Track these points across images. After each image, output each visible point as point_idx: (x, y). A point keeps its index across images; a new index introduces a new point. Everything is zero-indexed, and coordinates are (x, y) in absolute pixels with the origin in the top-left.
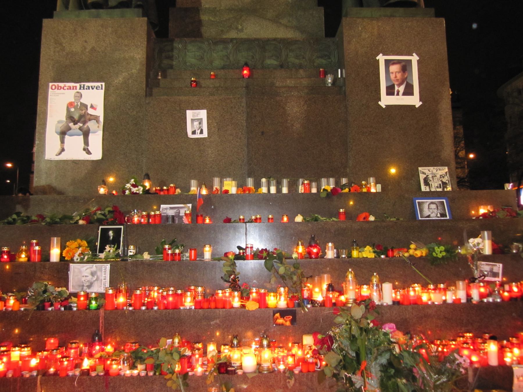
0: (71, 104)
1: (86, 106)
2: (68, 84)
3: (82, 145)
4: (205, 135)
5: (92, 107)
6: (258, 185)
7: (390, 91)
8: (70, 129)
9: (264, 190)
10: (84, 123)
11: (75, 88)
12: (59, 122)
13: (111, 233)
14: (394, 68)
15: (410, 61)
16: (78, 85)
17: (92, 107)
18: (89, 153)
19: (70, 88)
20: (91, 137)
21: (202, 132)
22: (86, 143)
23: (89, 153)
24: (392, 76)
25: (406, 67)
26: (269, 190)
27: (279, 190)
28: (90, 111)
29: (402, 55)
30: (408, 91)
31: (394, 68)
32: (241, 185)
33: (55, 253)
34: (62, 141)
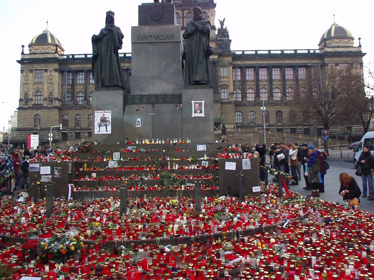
0: (101, 117)
1: (106, 118)
2: (100, 111)
3: (105, 129)
4: (140, 126)
5: (108, 118)
6: (155, 142)
7: (195, 112)
8: (101, 124)
9: (157, 142)
10: (106, 122)
11: (103, 112)
12: (99, 122)
13: (117, 154)
14: (197, 105)
15: (202, 103)
16: (103, 111)
17: (108, 118)
18: (107, 132)
19: (101, 112)
20: (108, 127)
21: (139, 125)
22: (106, 128)
23: (107, 132)
24: (196, 107)
25: (200, 104)
26: (159, 142)
27: (162, 142)
28: (107, 119)
29: (198, 101)
30: (201, 112)
31: (197, 105)
32: (150, 141)
33: (105, 160)
34: (100, 128)
